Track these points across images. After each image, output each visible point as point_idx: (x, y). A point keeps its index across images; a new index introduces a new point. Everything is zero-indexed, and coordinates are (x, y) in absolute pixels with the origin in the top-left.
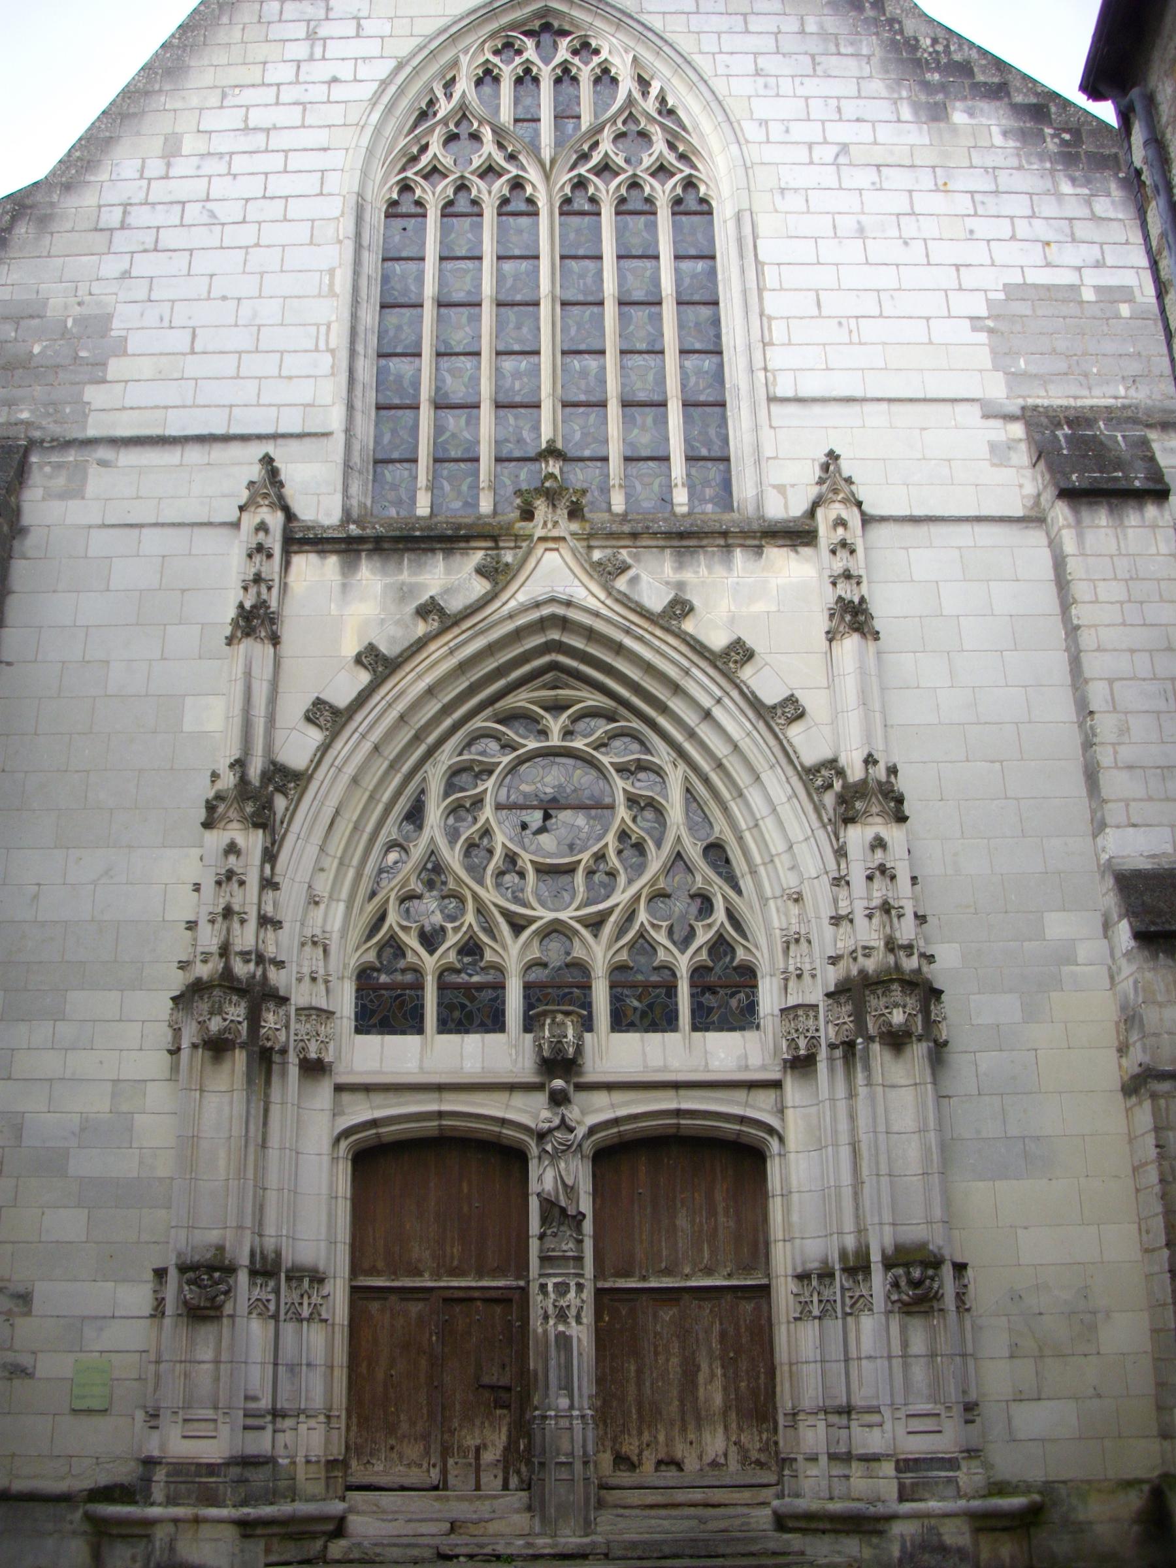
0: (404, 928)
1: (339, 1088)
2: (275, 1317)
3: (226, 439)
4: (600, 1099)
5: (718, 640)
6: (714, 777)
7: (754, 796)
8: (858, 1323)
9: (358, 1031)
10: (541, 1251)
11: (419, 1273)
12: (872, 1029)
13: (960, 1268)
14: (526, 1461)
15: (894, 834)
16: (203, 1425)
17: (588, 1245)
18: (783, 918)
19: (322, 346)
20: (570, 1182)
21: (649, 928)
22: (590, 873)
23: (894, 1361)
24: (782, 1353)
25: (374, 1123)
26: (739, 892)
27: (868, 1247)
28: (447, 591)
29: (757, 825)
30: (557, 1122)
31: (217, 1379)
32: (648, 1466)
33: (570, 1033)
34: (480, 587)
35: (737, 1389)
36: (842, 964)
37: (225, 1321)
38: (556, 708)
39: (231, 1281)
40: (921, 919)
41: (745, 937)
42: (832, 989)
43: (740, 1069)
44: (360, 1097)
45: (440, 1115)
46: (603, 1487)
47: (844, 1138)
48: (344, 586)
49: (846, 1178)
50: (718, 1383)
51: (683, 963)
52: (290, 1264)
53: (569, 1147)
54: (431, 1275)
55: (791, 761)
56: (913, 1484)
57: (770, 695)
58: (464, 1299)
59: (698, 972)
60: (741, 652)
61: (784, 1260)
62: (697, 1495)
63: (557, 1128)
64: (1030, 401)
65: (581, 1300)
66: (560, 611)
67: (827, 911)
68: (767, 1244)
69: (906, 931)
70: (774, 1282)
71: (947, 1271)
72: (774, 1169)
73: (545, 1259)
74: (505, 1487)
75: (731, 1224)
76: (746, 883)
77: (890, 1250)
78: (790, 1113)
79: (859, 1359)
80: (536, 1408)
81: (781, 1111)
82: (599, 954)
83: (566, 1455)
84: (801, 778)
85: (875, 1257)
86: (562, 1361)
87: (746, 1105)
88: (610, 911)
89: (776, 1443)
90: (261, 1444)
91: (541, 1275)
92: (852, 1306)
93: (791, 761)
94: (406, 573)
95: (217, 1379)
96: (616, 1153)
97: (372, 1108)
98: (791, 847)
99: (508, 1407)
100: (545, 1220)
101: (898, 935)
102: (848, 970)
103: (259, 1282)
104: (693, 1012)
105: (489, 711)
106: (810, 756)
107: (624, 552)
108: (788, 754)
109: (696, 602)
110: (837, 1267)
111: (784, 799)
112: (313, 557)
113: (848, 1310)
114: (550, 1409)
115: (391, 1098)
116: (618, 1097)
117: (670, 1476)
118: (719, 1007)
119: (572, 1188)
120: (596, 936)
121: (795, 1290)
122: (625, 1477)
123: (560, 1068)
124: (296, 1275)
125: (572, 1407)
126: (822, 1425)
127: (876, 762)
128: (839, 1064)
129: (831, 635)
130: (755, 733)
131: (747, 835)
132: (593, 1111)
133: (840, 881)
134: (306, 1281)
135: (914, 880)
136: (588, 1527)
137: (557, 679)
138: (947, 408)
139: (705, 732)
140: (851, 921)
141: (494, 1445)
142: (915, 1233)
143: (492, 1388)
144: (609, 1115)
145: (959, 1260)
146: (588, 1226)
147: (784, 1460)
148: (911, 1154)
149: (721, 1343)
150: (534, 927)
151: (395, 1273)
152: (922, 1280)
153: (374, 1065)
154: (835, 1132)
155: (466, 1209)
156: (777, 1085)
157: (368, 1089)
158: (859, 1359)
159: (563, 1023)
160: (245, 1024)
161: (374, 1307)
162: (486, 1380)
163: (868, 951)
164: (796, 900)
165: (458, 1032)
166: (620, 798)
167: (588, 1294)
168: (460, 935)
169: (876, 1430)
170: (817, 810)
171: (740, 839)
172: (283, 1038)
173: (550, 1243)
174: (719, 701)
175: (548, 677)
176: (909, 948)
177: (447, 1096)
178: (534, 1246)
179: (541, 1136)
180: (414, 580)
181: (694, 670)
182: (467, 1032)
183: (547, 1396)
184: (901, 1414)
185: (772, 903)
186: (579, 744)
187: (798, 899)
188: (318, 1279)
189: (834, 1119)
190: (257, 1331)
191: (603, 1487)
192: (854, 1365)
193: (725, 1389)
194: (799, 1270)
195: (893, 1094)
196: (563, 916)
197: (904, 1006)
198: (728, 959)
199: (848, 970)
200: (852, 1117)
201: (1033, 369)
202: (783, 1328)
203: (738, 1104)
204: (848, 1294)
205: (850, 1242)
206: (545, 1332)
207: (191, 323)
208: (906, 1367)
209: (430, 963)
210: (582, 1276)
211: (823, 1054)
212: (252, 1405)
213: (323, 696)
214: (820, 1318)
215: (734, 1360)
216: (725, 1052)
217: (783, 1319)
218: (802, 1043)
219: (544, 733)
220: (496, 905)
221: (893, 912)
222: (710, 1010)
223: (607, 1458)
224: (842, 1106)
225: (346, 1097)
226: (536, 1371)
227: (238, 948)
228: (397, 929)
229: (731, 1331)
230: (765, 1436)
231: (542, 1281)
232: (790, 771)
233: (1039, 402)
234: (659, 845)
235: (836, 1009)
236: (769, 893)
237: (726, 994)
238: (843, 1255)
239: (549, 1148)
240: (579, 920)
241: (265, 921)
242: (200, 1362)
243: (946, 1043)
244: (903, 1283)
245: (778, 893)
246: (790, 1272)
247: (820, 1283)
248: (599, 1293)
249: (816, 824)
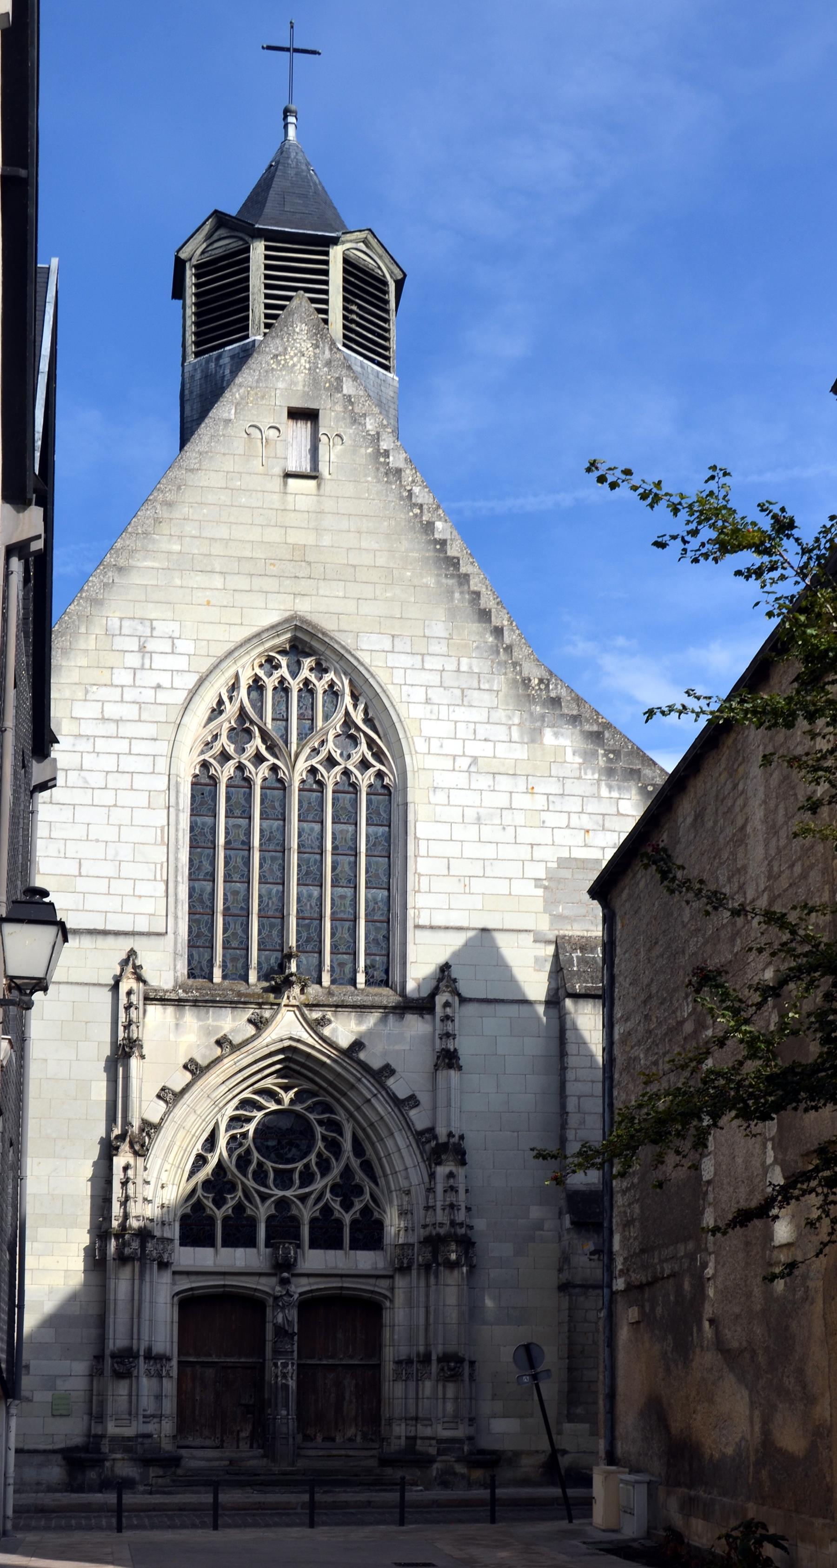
1: (174, 1273)
4: (304, 1280)
6: (369, 1130)
7: (390, 1143)
11: (210, 1355)
12: (440, 1260)
13: (472, 1363)
14: (263, 1436)
17: (295, 1348)
22: (301, 1173)
25: (192, 1289)
32: (319, 1439)
34: (251, 1030)
36: (428, 1229)
38: (286, 1088)
40: (468, 1209)
41: (378, 1206)
44: (184, 1277)
45: (224, 1286)
46: (299, 1448)
47: (422, 1304)
49: (422, 1321)
51: (347, 1218)
55: (410, 1128)
57: (402, 1095)
59: (354, 1222)
60: (388, 1070)
61: (389, 1354)
62: (343, 1452)
66: (294, 1044)
69: (461, 1216)
71: (466, 1366)
73: (277, 1352)
74: (251, 1447)
76: (382, 1181)
78: (396, 1291)
81: (392, 1289)
82: (306, 1213)
85: (434, 1357)
87: (375, 1285)
88: (311, 1193)
93: (410, 1128)
96: (310, 1305)
105: (250, 1089)
106: (420, 1126)
108: (409, 1124)
109: (366, 1043)
115: (200, 1278)
116: (312, 1280)
122: (309, 1444)
123: (283, 1267)
127: (454, 1136)
128: (422, 1272)
129: (436, 1067)
131: (384, 1160)
132: (300, 1287)
133: (431, 1190)
135: (467, 1191)
139: (366, 1109)
142: (452, 1348)
145: (473, 1359)
146: (296, 1338)
148: (452, 1316)
152: (455, 1366)
153: (191, 1262)
157: (188, 1273)
161: (189, 1370)
162: (243, 1402)
163: (441, 1225)
169: (429, 1429)
170: (421, 1154)
171: (380, 1159)
174: (375, 1095)
176: (461, 1225)
177: (227, 1277)
179: (276, 1298)
180: (215, 1023)
186: (298, 1108)
187: (408, 1193)
191: (299, 1448)
196: (288, 1193)
200: (427, 1296)
208: (444, 1403)
211: (415, 1266)
218: (405, 1261)
219: (279, 1102)
223: (299, 1437)
224: (422, 1290)
225: (177, 1277)
232: (409, 1134)
234: (337, 1160)
236: (393, 1187)
237: (369, 1234)
238: (418, 1355)
240: (295, 1196)
248: (299, 1365)
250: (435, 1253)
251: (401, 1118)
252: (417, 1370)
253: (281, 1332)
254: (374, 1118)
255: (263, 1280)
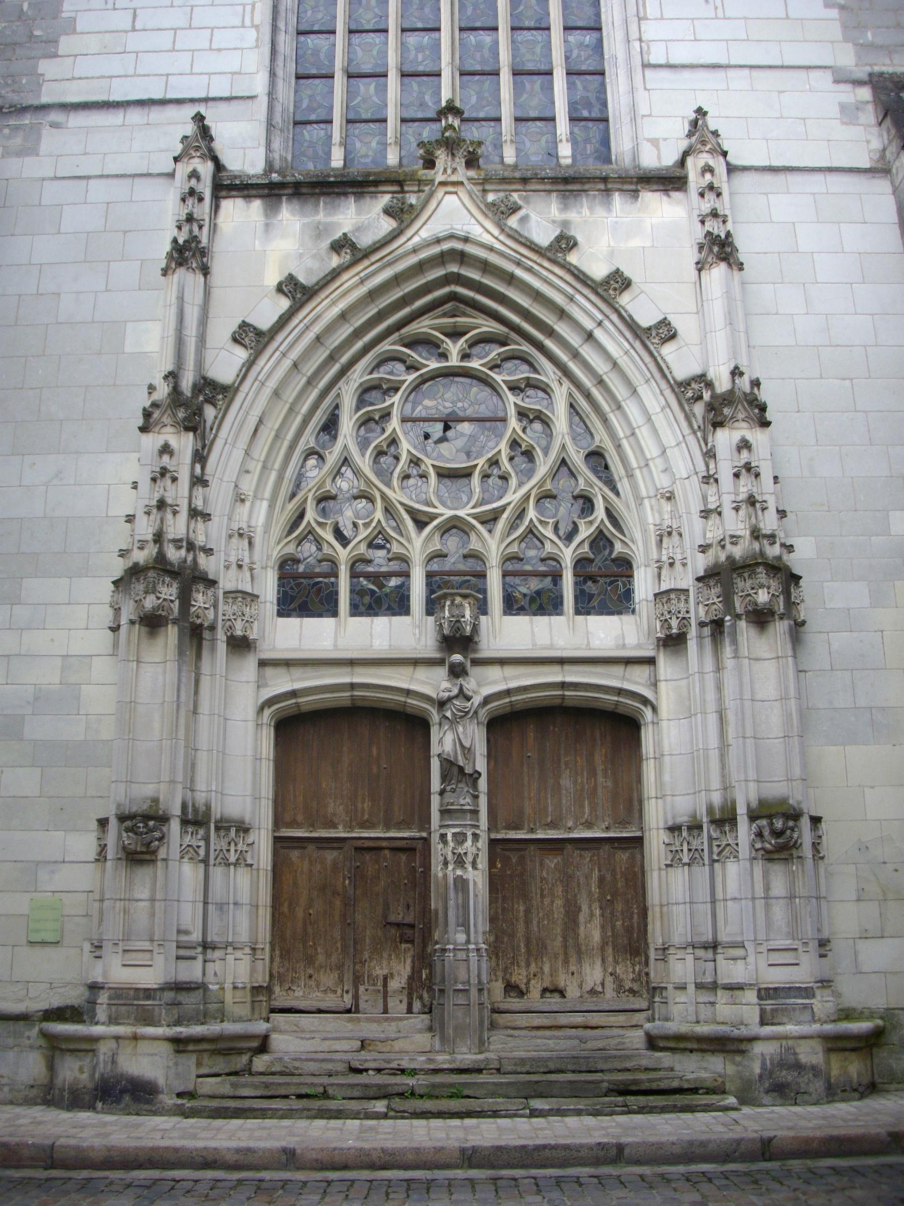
0: (320, 524)
2: (205, 861)
3: (163, 102)
4: (494, 672)
5: (599, 271)
6: (596, 393)
7: (632, 409)
8: (724, 869)
9: (280, 614)
10: (442, 805)
11: (334, 826)
12: (739, 607)
13: (816, 821)
14: (427, 989)
15: (757, 436)
16: (141, 955)
17: (483, 801)
18: (657, 515)
19: (248, 22)
20: (467, 745)
21: (537, 524)
22: (486, 476)
23: (757, 902)
24: (654, 896)
25: (294, 694)
26: (617, 494)
27: (734, 803)
28: (358, 229)
29: (633, 434)
30: (455, 691)
31: (153, 915)
32: (535, 993)
33: (468, 613)
34: (387, 225)
35: (613, 928)
36: (711, 552)
37: (159, 864)
38: (455, 334)
39: (165, 829)
40: (782, 514)
41: (622, 532)
42: (702, 573)
43: (617, 648)
44: (281, 671)
45: (353, 686)
46: (495, 1011)
47: (712, 706)
48: (267, 225)
49: (713, 742)
50: (597, 921)
51: (568, 555)
52: (218, 816)
53: (467, 713)
54: (345, 827)
55: (664, 376)
56: (772, 1010)
57: (646, 319)
58: (372, 848)
59: (581, 563)
60: (619, 282)
61: (656, 816)
62: (578, 1019)
63: (456, 697)
64: (877, 69)
65: (477, 848)
66: (459, 246)
67: (696, 507)
68: (641, 802)
69: (769, 522)
70: (647, 835)
71: (805, 823)
72: (647, 736)
74: (410, 1010)
75: (609, 784)
76: (624, 486)
77: (754, 804)
78: (662, 686)
79: (725, 900)
80: (437, 943)
81: (655, 685)
82: (493, 546)
83: (463, 983)
84: (673, 390)
85: (741, 810)
86: (460, 901)
87: (623, 678)
88: (503, 509)
89: (647, 974)
90: (192, 971)
91: (441, 827)
92: (719, 854)
93: (664, 376)
94: (322, 214)
95: (153, 915)
96: (509, 722)
97: (292, 681)
98: (664, 452)
99: (412, 942)
100: (444, 778)
101: (762, 525)
102: (717, 557)
103: (190, 830)
104: (576, 597)
105: (395, 336)
106: (681, 372)
107: (515, 196)
109: (580, 239)
110: (705, 819)
111: (658, 410)
112: (240, 202)
113: (715, 857)
114: (448, 943)
115: (309, 671)
116: (509, 671)
117: (554, 1001)
118: (599, 594)
119: (469, 749)
120: (490, 531)
121: (667, 841)
122: (515, 1003)
123: (458, 643)
124: (223, 825)
125: (468, 942)
126: (690, 958)
127: (741, 374)
128: (708, 641)
129: (700, 266)
130: (632, 351)
131: (625, 443)
132: (487, 683)
133: (709, 479)
134: (233, 830)
136: (482, 1045)
137: (454, 310)
138: (802, 74)
139: (587, 352)
140: (720, 514)
141: (399, 974)
142: (775, 790)
143: (398, 925)
144: (502, 687)
145: (814, 814)
146: (483, 784)
147: (655, 988)
148: (773, 721)
149: (599, 888)
150: (435, 523)
151: (312, 825)
152: (782, 831)
153: (293, 643)
154: (704, 701)
155: (375, 770)
156: (651, 661)
157: (288, 664)
158: (725, 900)
159: (461, 605)
160: (177, 603)
161: (295, 855)
162: (392, 918)
163: (735, 539)
164: (669, 499)
165: (369, 615)
166: (512, 412)
167: (483, 843)
168: (370, 529)
170: (687, 418)
171: (619, 447)
172: (211, 615)
173: (449, 797)
174: (600, 324)
175: (448, 307)
176: (772, 537)
177: (359, 670)
178: (435, 801)
179: (442, 704)
180: (329, 219)
181: (578, 297)
182: (376, 615)
183: (446, 932)
184: (763, 949)
185: (646, 502)
187: (670, 497)
188: (243, 829)
189: (703, 690)
190: (189, 874)
191: (495, 1011)
192: (720, 906)
193: (603, 927)
194: (670, 823)
195: (757, 666)
196: (461, 513)
197: (768, 588)
198: (607, 552)
199: (717, 557)
200: (719, 688)
201: (879, 41)
202: (655, 874)
203: (616, 678)
204: (715, 843)
205: (717, 798)
206: (445, 876)
207: (133, 5)
208: (768, 907)
209: (343, 555)
210: (477, 827)
211: (693, 632)
212: (183, 938)
213: (247, 320)
214: (689, 865)
215: (611, 902)
216: (604, 633)
217: (655, 866)
218: (674, 623)
219: (444, 356)
220: (402, 504)
221: (758, 505)
222: (591, 597)
223: (498, 987)
224: (710, 680)
225: (269, 671)
226: (436, 911)
227: (171, 536)
228: (314, 525)
229: (608, 877)
230: (637, 968)
231: (443, 831)
232: (663, 385)
233: (884, 69)
235: (706, 592)
236: (644, 493)
237: (605, 582)
238: (710, 810)
239: (448, 714)
240: (476, 517)
241: (194, 513)
242: (137, 900)
243: (803, 623)
244: (766, 833)
245: (652, 494)
246: (661, 825)
247: (690, 835)
248: (493, 843)
249: (687, 431)
250: (727, 599)
251: (647, 359)
252: (710, 839)
253: (454, 772)
254: (601, 366)
255: (422, 673)
